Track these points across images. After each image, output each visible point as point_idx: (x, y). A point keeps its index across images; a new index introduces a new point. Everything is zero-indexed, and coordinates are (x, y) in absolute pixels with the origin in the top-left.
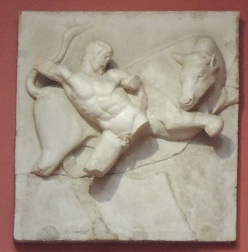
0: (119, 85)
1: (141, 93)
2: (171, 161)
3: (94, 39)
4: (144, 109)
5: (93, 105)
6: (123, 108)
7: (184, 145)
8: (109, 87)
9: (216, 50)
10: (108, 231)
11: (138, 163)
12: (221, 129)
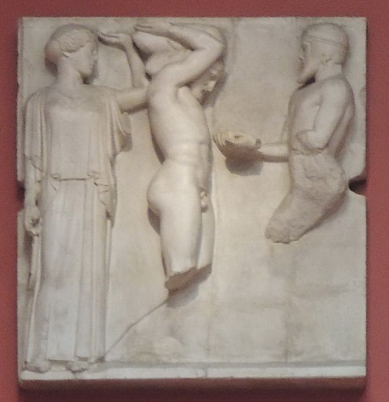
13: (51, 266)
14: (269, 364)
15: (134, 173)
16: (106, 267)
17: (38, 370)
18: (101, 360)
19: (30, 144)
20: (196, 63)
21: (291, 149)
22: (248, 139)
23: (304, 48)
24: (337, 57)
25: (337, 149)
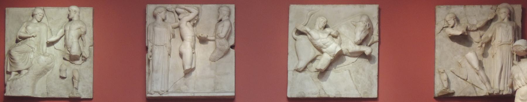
0: (330, 34)
1: (339, 38)
2: (351, 65)
3: (320, 16)
4: (340, 44)
5: (319, 42)
6: (331, 44)
7: (356, 59)
8: (326, 35)
9: (369, 20)
10: (325, 93)
11: (338, 66)
12: (371, 52)
13: (155, 68)
14: (210, 92)
15: (176, 43)
16: (168, 67)
17: (151, 94)
18: (167, 91)
19: (149, 37)
20: (191, 16)
21: (216, 38)
22: (205, 35)
23: (219, 12)
24: (227, 15)
25: (228, 38)
